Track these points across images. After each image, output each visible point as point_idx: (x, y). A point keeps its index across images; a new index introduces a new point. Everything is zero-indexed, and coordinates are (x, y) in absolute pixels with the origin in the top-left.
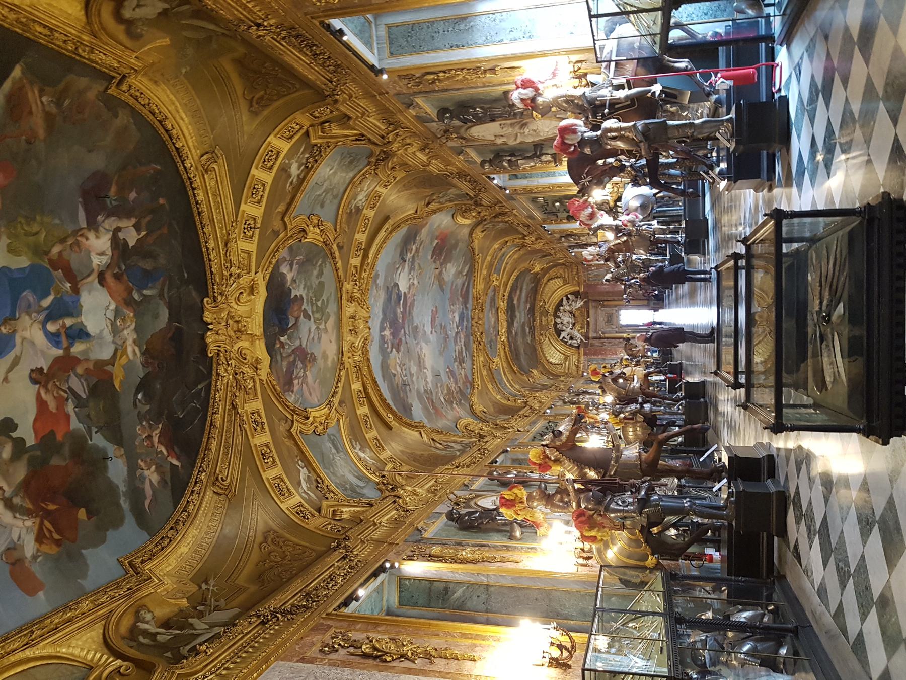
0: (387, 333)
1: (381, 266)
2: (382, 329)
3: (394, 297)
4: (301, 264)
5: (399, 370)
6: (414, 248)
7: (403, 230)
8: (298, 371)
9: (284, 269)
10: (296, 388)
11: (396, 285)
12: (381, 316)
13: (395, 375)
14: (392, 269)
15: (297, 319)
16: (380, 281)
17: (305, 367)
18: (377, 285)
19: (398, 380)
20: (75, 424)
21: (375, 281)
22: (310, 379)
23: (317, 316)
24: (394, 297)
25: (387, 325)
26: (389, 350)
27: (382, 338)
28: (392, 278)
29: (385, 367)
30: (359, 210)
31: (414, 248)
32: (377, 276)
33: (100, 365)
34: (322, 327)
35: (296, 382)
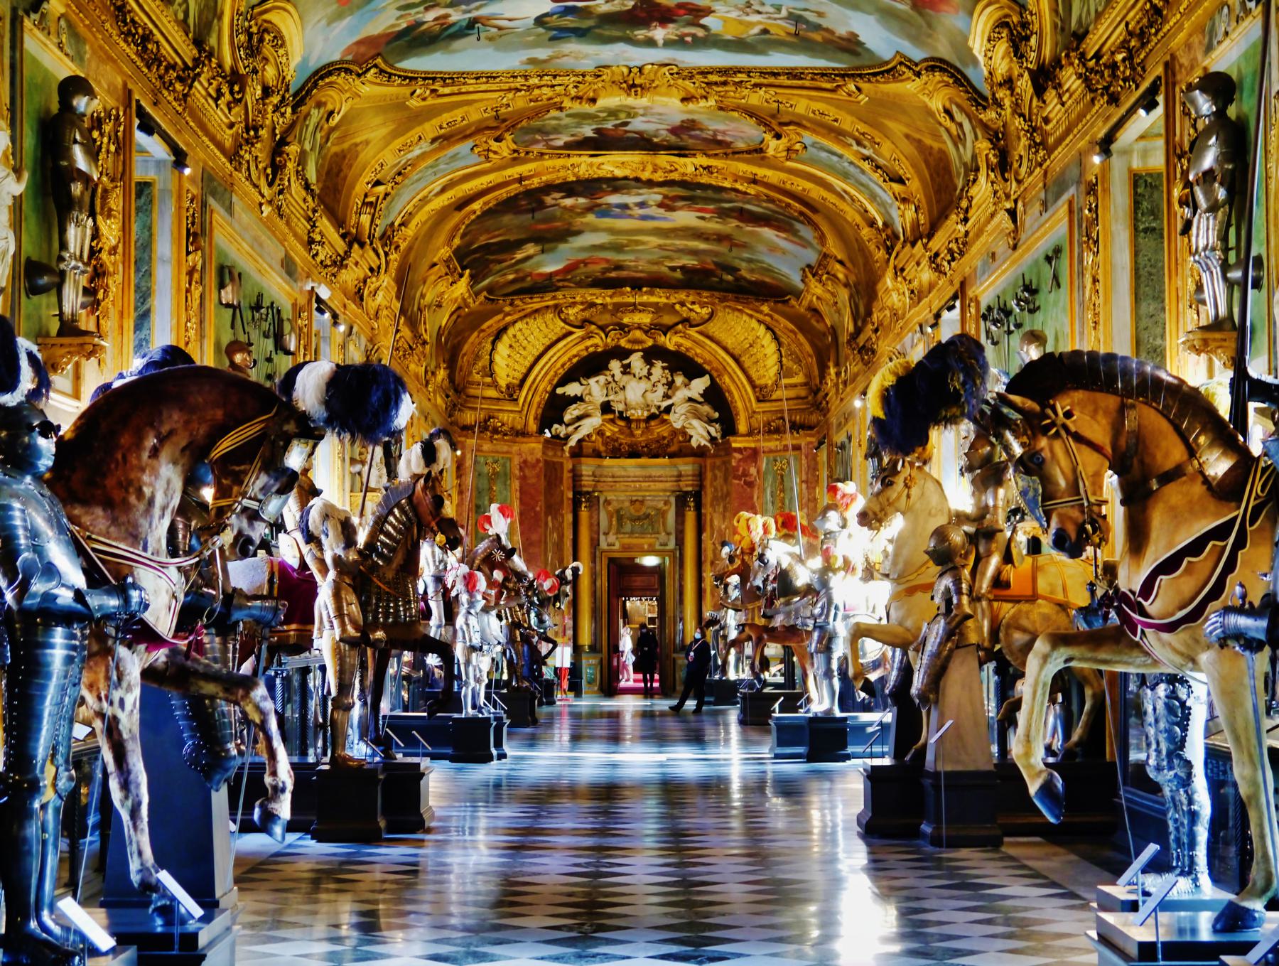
0: (659, 33)
1: (510, 61)
2: (651, 43)
3: (570, 21)
4: (547, 133)
5: (755, 18)
6: (430, 16)
7: (414, 63)
8: (708, 135)
9: (560, 143)
10: (728, 139)
11: (540, 21)
12: (620, 47)
13: (765, 31)
14: (503, 36)
15: (627, 132)
16: (542, 54)
17: (701, 130)
18: (551, 58)
19: (781, 28)
20: (712, 207)
21: (545, 61)
22: (721, 127)
23: (622, 116)
24: (570, 21)
25: (641, 34)
26: (700, 33)
27: (668, 44)
28: (528, 32)
29: (740, 45)
30: (434, 140)
31: (430, 16)
32: (533, 61)
33: (665, 197)
34: (641, 112)
35: (719, 138)
